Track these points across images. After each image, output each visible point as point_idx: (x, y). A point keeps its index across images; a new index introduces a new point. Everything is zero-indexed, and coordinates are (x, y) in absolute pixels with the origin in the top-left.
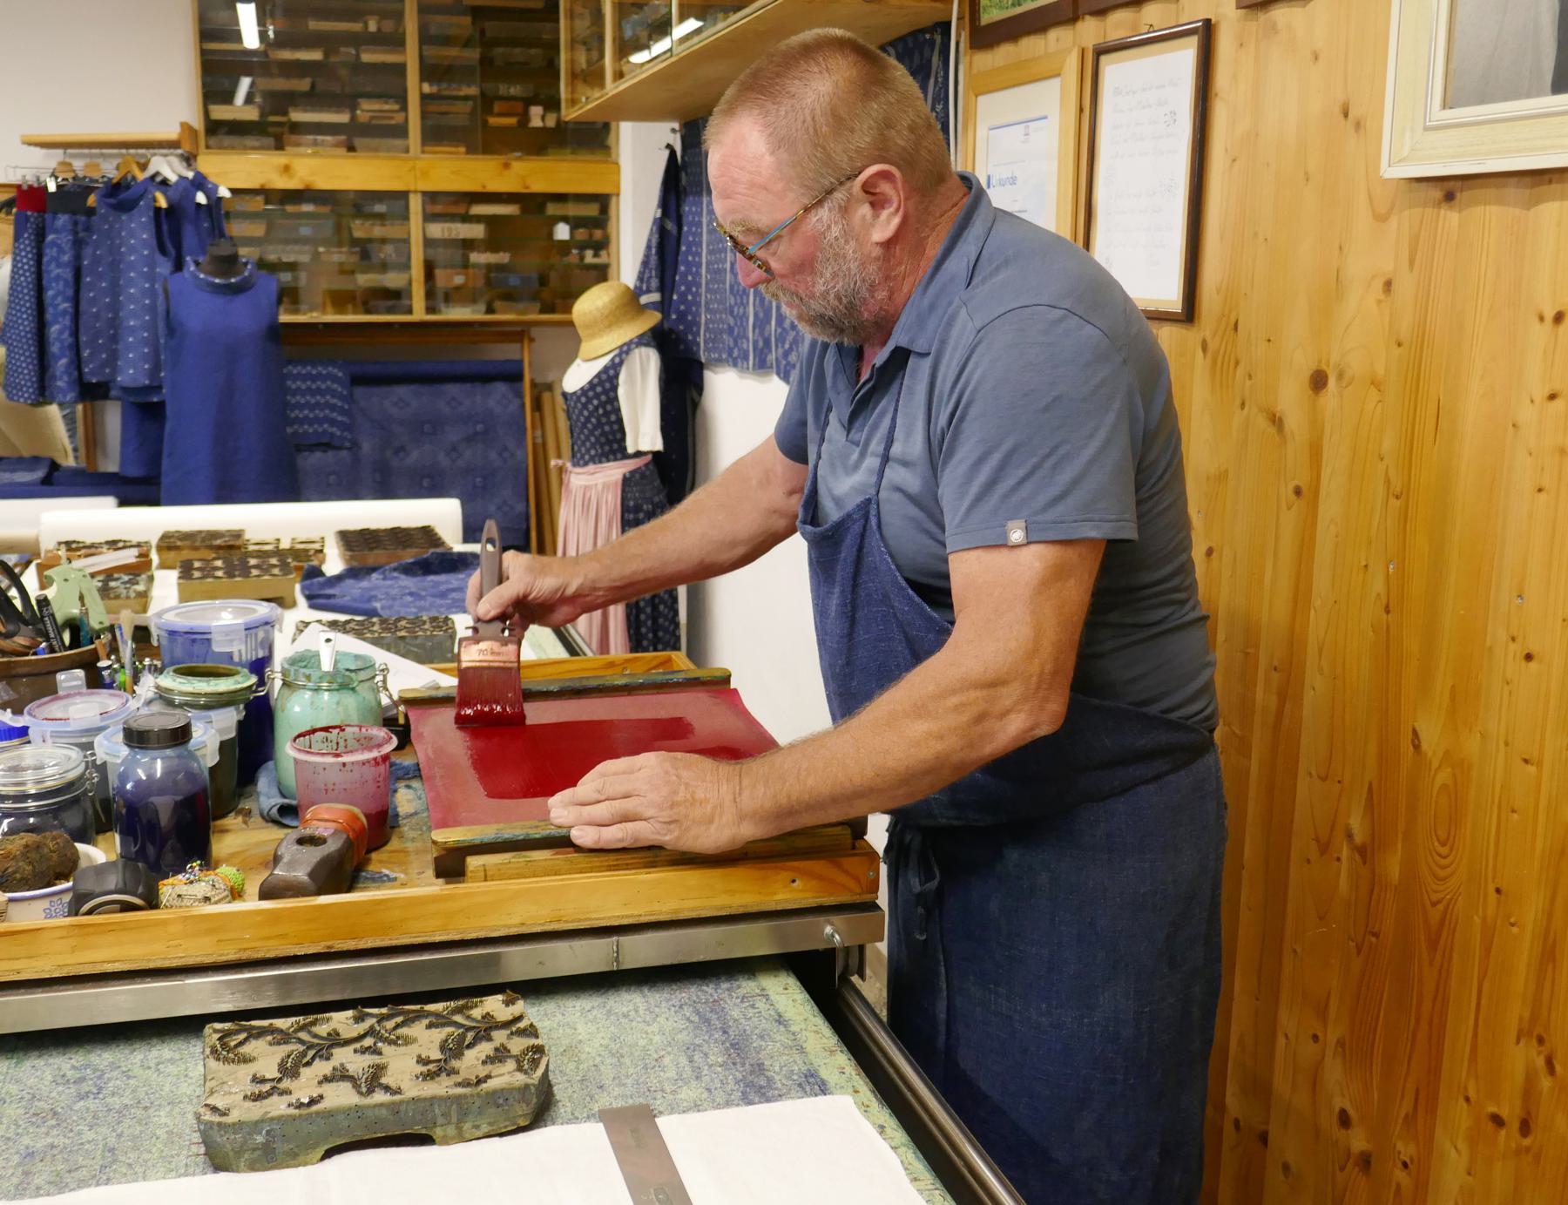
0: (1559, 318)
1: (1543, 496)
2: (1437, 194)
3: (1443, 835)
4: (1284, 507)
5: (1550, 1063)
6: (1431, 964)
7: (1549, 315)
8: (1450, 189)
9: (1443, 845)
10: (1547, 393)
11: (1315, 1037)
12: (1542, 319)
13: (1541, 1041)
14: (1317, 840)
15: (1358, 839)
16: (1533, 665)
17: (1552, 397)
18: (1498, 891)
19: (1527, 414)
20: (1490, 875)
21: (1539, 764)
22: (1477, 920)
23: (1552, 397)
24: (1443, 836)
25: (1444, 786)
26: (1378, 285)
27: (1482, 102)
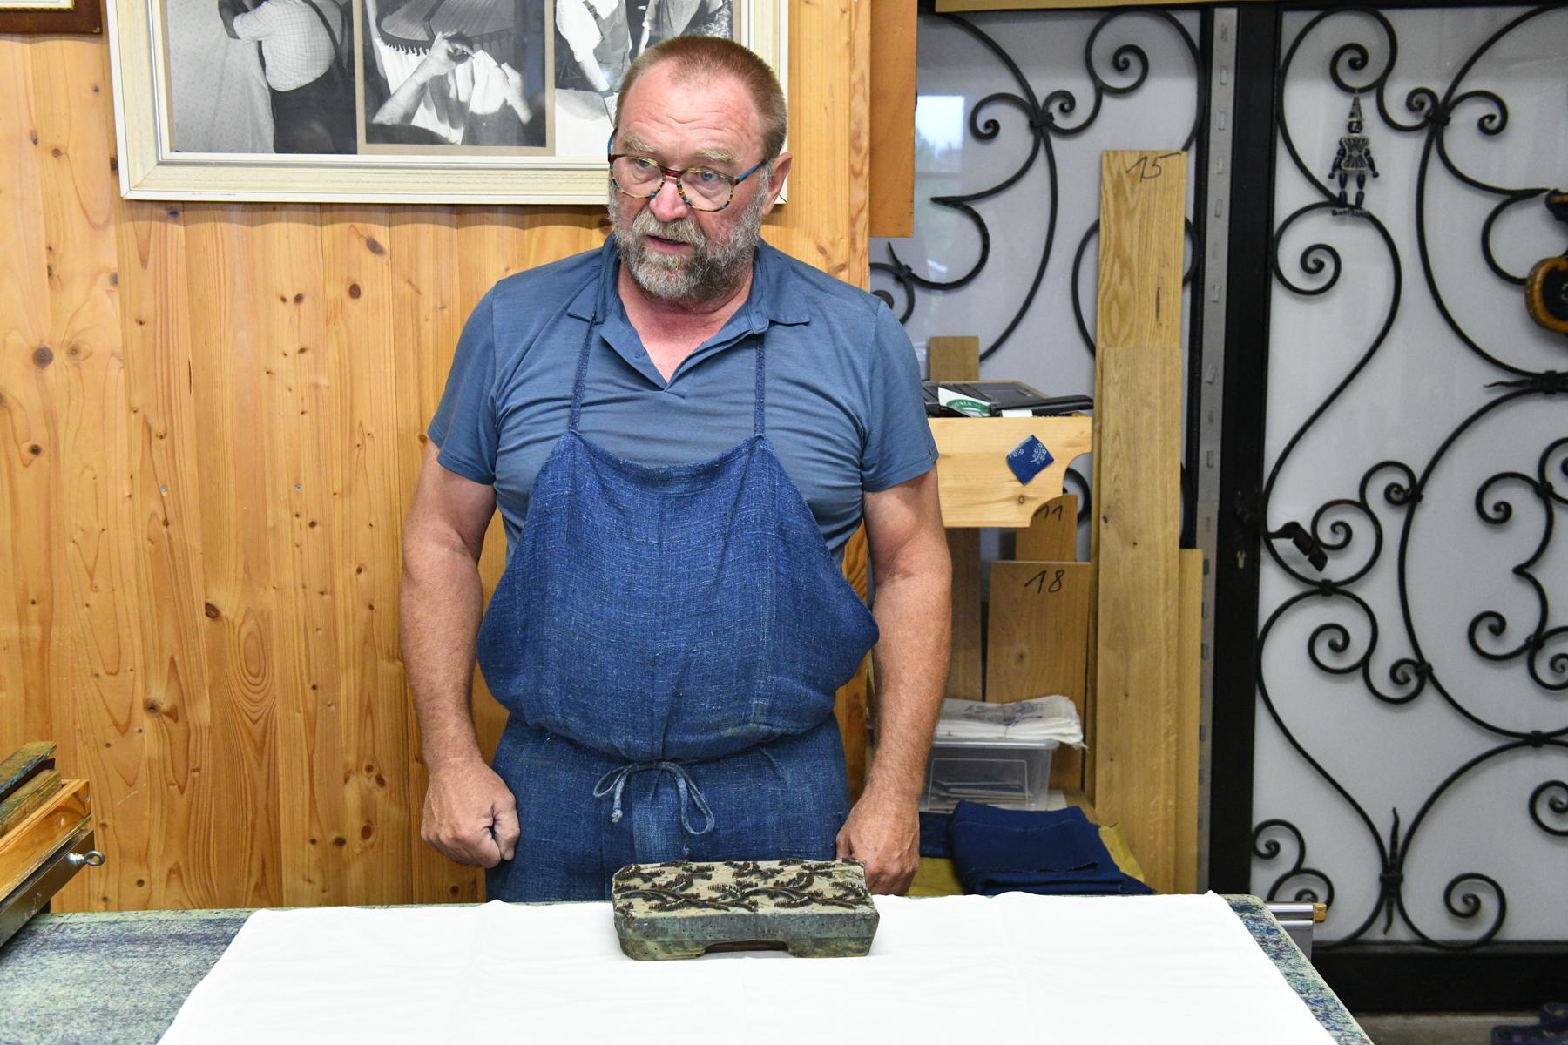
0: (299, 299)
1: (307, 416)
2: (163, 212)
3: (254, 669)
4: (18, 465)
5: (380, 781)
6: (260, 765)
7: (290, 297)
8: (175, 210)
9: (256, 676)
10: (298, 347)
11: (140, 883)
12: (284, 300)
13: (369, 769)
14: (116, 724)
15: (165, 706)
16: (317, 529)
17: (302, 351)
18: (314, 687)
19: (279, 364)
20: (305, 678)
21: (332, 592)
22: (299, 717)
23: (302, 351)
24: (254, 669)
25: (249, 634)
26: (104, 279)
27: (210, 151)
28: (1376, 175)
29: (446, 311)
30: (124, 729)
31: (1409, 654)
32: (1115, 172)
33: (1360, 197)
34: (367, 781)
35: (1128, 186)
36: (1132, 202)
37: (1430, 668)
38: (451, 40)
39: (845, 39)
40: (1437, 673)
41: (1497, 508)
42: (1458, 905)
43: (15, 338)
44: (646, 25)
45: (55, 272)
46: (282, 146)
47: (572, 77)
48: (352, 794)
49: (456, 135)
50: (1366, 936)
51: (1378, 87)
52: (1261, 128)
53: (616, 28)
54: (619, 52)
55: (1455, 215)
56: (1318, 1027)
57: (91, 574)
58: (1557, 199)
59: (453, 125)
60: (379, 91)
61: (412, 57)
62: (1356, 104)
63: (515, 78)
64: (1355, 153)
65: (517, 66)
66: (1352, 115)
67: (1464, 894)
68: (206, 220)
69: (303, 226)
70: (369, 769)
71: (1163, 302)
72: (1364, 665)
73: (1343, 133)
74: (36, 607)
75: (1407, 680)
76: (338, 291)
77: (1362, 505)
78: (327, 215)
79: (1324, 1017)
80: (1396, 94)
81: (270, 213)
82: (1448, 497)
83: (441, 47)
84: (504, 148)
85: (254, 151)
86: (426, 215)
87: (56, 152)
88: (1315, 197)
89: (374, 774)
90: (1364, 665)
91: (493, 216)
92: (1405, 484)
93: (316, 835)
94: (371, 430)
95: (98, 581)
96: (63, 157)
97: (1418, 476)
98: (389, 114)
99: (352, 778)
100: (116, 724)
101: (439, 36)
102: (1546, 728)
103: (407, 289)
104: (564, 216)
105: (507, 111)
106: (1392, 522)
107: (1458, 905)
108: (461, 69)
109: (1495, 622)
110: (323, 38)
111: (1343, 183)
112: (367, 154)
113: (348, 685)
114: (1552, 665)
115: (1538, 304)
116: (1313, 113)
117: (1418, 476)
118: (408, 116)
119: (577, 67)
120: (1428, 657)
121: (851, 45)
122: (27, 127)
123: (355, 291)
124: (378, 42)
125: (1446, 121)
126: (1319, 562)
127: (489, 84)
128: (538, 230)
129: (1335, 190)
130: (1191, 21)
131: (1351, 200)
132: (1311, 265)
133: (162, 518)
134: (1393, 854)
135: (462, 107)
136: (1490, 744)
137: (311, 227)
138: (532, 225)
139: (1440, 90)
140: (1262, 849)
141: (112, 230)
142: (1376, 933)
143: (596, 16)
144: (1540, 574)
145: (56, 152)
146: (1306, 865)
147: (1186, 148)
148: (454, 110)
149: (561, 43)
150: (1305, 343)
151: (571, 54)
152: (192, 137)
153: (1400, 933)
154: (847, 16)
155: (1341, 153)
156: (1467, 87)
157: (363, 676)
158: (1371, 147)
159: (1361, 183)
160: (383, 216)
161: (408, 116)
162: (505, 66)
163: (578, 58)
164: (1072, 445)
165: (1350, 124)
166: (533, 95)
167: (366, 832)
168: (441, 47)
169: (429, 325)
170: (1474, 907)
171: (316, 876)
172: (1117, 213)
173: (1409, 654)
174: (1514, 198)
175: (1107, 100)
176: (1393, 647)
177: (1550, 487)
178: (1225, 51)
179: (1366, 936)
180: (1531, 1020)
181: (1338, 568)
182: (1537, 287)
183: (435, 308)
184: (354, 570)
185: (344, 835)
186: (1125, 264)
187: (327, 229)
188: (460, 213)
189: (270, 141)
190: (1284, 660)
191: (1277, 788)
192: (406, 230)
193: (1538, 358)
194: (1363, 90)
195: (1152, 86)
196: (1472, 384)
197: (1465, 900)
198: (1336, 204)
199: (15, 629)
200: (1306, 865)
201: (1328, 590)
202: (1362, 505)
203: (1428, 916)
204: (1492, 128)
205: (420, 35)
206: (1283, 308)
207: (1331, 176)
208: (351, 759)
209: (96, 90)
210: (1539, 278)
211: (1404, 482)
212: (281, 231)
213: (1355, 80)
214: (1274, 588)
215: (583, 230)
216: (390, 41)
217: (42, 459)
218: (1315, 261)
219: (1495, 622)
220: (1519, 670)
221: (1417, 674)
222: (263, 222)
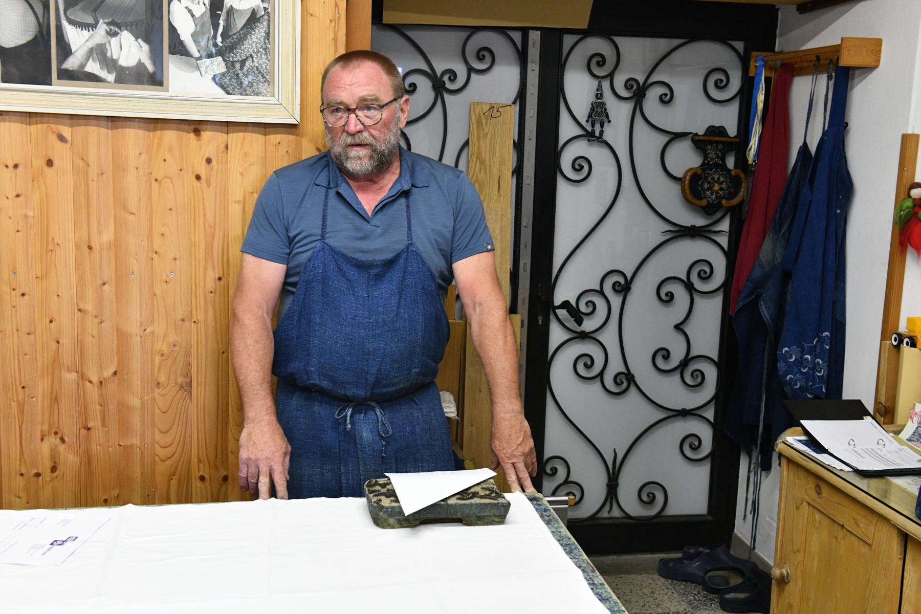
0: (16, 166)
1: (20, 233)
5: (63, 440)
7: (11, 165)
10: (15, 194)
12: (7, 166)
13: (56, 433)
16: (26, 297)
17: (18, 196)
18: (23, 387)
20: (18, 382)
21: (35, 334)
22: (14, 404)
23: (18, 196)
28: (609, 122)
29: (104, 176)
31: (624, 370)
32: (477, 113)
33: (602, 133)
34: (54, 440)
35: (484, 121)
36: (486, 130)
37: (633, 376)
38: (108, 24)
39: (332, 36)
40: (636, 379)
41: (667, 295)
42: (645, 498)
44: (221, 22)
47: (178, 48)
48: (45, 448)
49: (111, 78)
50: (599, 515)
51: (611, 76)
52: (552, 95)
55: (648, 144)
56: (566, 558)
58: (697, 138)
59: (109, 72)
60: (65, 51)
61: (85, 32)
62: (600, 84)
63: (145, 47)
64: (599, 110)
65: (147, 41)
66: (598, 90)
67: (649, 491)
70: (56, 433)
71: (501, 184)
72: (601, 375)
73: (593, 99)
75: (622, 383)
76: (40, 163)
77: (601, 292)
78: (33, 119)
79: (569, 552)
80: (620, 80)
82: (644, 288)
83: (102, 28)
86: (92, 122)
88: (578, 132)
89: (59, 436)
90: (601, 375)
92: (622, 281)
93: (24, 471)
94: (60, 242)
97: (629, 277)
98: (71, 63)
99: (46, 439)
101: (101, 21)
102: (688, 407)
103: (82, 163)
104: (173, 126)
105: (140, 65)
106: (616, 301)
107: (645, 498)
108: (114, 41)
109: (665, 353)
110: (32, 19)
111: (593, 125)
112: (58, 86)
113: (42, 387)
114: (692, 375)
115: (687, 191)
116: (578, 88)
117: (629, 277)
118: (83, 65)
119: (181, 43)
120: (632, 372)
121: (335, 39)
123: (50, 163)
124: (65, 23)
125: (644, 96)
126: (579, 322)
127: (130, 50)
128: (158, 132)
129: (589, 129)
130: (517, 36)
131: (597, 134)
132: (577, 167)
134: (614, 472)
135: (114, 62)
136: (661, 415)
137: (24, 126)
138: (155, 130)
139: (641, 79)
140: (549, 471)
142: (605, 514)
143: (193, 16)
144: (687, 329)
146: (571, 479)
147: (514, 103)
148: (110, 64)
150: (574, 207)
151: (178, 35)
153: (616, 513)
154: (333, 24)
155: (592, 109)
157: (52, 380)
158: (607, 106)
159: (602, 126)
160: (68, 121)
161: (83, 65)
162: (140, 40)
163: (182, 39)
165: (597, 95)
166: (156, 56)
167: (54, 469)
168: (102, 28)
169: (94, 182)
170: (652, 499)
171: (23, 495)
172: (479, 138)
173: (624, 370)
174: (676, 136)
175: (473, 75)
176: (615, 366)
177: (692, 284)
178: (534, 53)
179: (599, 515)
180: (679, 555)
181: (589, 325)
182: (687, 182)
183: (98, 174)
184: (48, 322)
185: (40, 471)
186: (482, 163)
187: (33, 127)
188: (113, 121)
190: (561, 373)
191: (558, 438)
192: (81, 130)
194: (603, 77)
195: (497, 69)
196: (656, 231)
197: (648, 495)
198: (590, 136)
200: (571, 479)
201: (584, 336)
202: (601, 292)
203: (630, 503)
204: (666, 100)
205: (90, 20)
206: (563, 190)
207: (587, 121)
208: (46, 428)
210: (688, 178)
211: (622, 281)
213: (598, 72)
214: (557, 335)
215: (185, 134)
218: (579, 165)
219: (665, 353)
220: (676, 378)
221: (627, 380)
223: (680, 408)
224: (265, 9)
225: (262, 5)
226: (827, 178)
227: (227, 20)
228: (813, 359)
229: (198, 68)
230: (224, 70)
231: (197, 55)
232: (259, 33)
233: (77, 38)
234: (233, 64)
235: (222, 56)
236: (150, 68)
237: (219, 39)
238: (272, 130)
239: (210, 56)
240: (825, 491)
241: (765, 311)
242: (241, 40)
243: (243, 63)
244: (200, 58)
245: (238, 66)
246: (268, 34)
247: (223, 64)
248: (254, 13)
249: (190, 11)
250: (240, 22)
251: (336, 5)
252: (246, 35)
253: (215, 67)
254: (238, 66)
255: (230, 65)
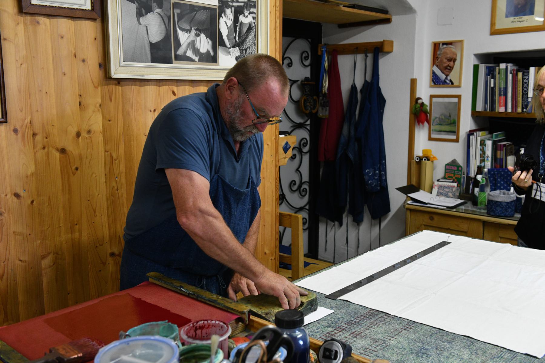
0: (155, 111)
4: (71, 174)
7: (152, 110)
12: (151, 111)
14: (103, 263)
15: (117, 253)
30: (104, 264)
37: (285, 196)
38: (196, 30)
40: (286, 197)
43: (70, 128)
45: (82, 104)
46: (153, 61)
49: (197, 59)
53: (231, 30)
54: (232, 37)
57: (95, 212)
59: (196, 56)
60: (178, 45)
61: (186, 34)
63: (210, 42)
65: (211, 39)
68: (129, 85)
69: (155, 87)
74: (77, 226)
81: (147, 83)
84: (207, 63)
85: (145, 62)
87: (83, 61)
91: (202, 84)
95: (97, 213)
96: (86, 63)
98: (180, 52)
100: (103, 263)
108: (198, 39)
110: (163, 26)
112: (176, 65)
118: (185, 53)
122: (74, 52)
124: (178, 29)
127: (204, 44)
133: (116, 188)
135: (198, 50)
141: (99, 88)
145: (83, 61)
148: (196, 51)
149: (220, 33)
152: (130, 57)
156: (285, 56)
160: (205, 84)
164: (293, 143)
168: (193, 32)
174: (293, 82)
189: (150, 59)
193: (298, 120)
199: (70, 236)
204: (290, 65)
205: (188, 28)
209: (95, 39)
212: (150, 89)
216: (181, 29)
217: (79, 172)
222: (144, 86)
223: (298, 207)
224: (254, 23)
225: (253, 21)
226: (372, 97)
227: (240, 29)
228: (380, 172)
229: (229, 53)
230: (239, 54)
231: (229, 46)
232: (252, 35)
233: (184, 38)
234: (243, 50)
235: (238, 46)
236: (212, 54)
237: (237, 38)
238: (183, 83)
239: (233, 47)
240: (436, 218)
241: (351, 156)
242: (245, 39)
243: (246, 50)
244: (229, 48)
245: (244, 52)
246: (255, 35)
247: (239, 51)
248: (250, 25)
249: (226, 23)
250: (245, 30)
251: (276, 22)
252: (247, 36)
253: (236, 53)
254: (244, 52)
255: (241, 51)
